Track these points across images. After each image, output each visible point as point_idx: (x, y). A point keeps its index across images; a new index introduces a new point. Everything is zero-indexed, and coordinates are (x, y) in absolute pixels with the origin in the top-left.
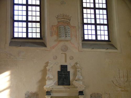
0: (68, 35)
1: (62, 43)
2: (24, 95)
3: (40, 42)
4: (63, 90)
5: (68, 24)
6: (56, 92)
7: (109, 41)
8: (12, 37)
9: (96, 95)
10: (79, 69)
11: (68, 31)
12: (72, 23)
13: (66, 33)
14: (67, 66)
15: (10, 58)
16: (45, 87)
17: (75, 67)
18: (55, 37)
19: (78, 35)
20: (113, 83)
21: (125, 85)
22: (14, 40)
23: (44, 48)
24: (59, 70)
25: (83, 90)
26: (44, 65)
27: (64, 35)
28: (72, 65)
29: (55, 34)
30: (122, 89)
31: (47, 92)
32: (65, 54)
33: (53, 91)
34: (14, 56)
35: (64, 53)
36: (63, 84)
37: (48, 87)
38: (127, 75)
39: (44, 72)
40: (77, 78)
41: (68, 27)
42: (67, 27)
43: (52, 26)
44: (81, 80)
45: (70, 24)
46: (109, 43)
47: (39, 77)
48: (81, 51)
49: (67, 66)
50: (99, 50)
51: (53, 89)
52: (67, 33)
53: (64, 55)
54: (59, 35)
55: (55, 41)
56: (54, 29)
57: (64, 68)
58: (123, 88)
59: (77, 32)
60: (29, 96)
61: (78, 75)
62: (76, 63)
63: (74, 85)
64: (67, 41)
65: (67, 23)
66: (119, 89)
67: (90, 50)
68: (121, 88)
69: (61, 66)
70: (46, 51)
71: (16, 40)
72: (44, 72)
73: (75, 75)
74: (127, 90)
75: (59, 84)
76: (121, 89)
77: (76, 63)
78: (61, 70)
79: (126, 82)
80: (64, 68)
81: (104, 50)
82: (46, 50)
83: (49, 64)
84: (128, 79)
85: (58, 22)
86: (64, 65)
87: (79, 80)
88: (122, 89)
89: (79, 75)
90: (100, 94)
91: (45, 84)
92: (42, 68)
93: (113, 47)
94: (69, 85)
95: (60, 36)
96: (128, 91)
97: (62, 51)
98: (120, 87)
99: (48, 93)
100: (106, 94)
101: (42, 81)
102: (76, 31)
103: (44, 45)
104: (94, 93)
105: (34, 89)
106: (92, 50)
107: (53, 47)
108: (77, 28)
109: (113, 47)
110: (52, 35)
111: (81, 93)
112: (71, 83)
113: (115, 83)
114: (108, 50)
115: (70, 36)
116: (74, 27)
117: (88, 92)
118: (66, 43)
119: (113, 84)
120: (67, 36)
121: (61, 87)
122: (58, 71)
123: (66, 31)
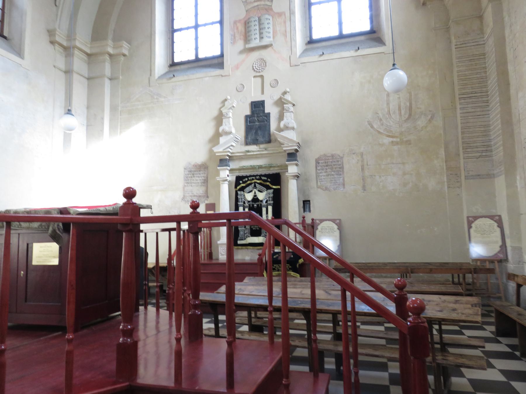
0: (265, 34)
1: (255, 55)
2: (183, 170)
3: (217, 62)
4: (255, 153)
5: (268, 9)
6: (240, 158)
7: (372, 32)
8: (171, 63)
9: (328, 159)
10: (290, 106)
11: (267, 26)
12: (276, 7)
13: (262, 31)
14: (263, 102)
15: (158, 101)
16: (215, 149)
17: (281, 103)
18: (240, 45)
19: (288, 29)
20: (372, 127)
21: (403, 130)
22: (173, 68)
23: (218, 72)
24: (248, 113)
25: (297, 151)
26: (219, 106)
27: (258, 36)
28: (276, 97)
29: (240, 39)
30: (395, 140)
31: (221, 160)
32: (262, 77)
33: (235, 158)
34: (165, 97)
35: (258, 74)
36: (255, 142)
37: (221, 150)
38: (408, 104)
39: (219, 119)
40: (282, 124)
41: (267, 16)
42: (263, 18)
43: (235, 22)
44: (293, 129)
45: (272, 9)
46: (374, 35)
47: (210, 132)
48: (296, 66)
49: (264, 101)
50: (336, 55)
51: (231, 153)
52: (264, 31)
53: (259, 80)
54: (247, 39)
55: (241, 52)
56: (237, 28)
57: (257, 107)
58: (397, 137)
59: (288, 23)
60: (191, 171)
61: (285, 118)
62: (285, 93)
63: (278, 141)
64: (265, 47)
65: (266, 9)
66: (387, 140)
67: (315, 58)
68: (392, 137)
69: (252, 103)
70: (223, 78)
71: (178, 68)
72: (219, 119)
73: (281, 118)
74: (407, 141)
75: (247, 144)
76: (391, 139)
77: (285, 93)
78: (253, 112)
79: (406, 120)
80: (257, 107)
81: (352, 53)
82: (222, 76)
83: (226, 103)
84: (410, 115)
85: (247, 11)
86: (258, 102)
87: (287, 128)
88: (395, 140)
89: (289, 119)
90: (339, 156)
91: (218, 143)
92: (215, 113)
93: (380, 41)
94: (269, 142)
95: (249, 41)
96: (410, 144)
97: (255, 71)
98: (388, 136)
99: (223, 162)
100: (354, 154)
101: (215, 139)
102: (285, 22)
103: (221, 65)
104: (325, 155)
105: (200, 156)
106: (322, 58)
107: (237, 67)
108: (287, 14)
109: (380, 41)
110: (234, 41)
111: (292, 156)
112: (272, 138)
113: (375, 127)
114: (359, 51)
115: (271, 35)
116: (280, 14)
117: (311, 154)
118: (263, 53)
119: (371, 129)
120: (263, 38)
121: (253, 148)
122: (247, 117)
123: (262, 26)
